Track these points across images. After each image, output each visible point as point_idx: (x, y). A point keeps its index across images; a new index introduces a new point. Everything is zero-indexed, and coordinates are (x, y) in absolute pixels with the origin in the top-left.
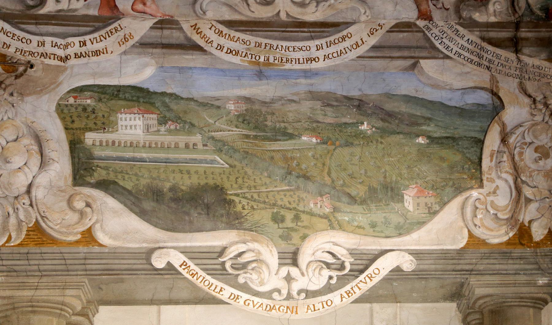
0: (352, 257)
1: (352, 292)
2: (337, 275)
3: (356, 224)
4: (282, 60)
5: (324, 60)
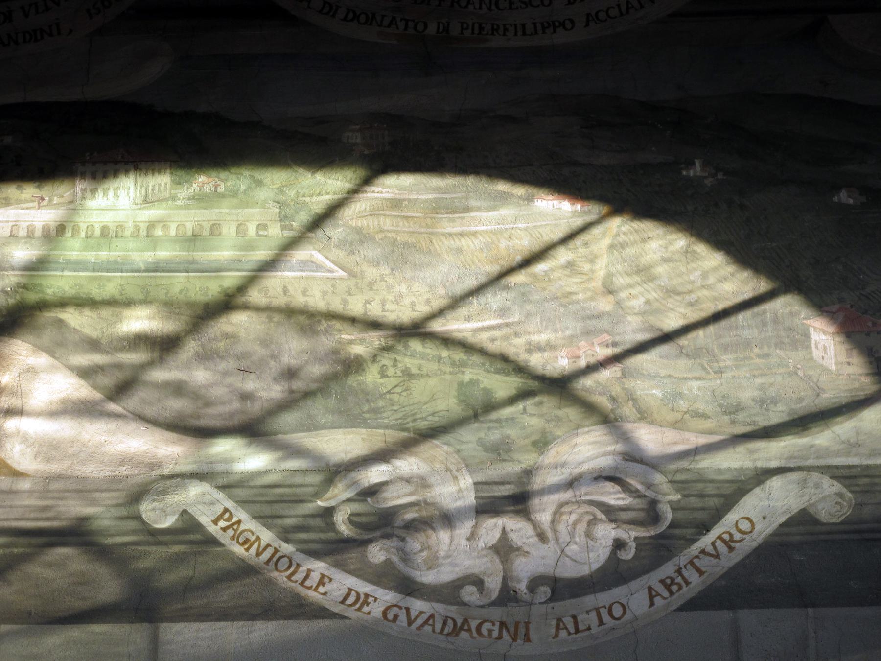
0: (678, 491)
1: (679, 580)
2: (636, 539)
3: (683, 405)
4: (481, 29)
5: (587, 25)
